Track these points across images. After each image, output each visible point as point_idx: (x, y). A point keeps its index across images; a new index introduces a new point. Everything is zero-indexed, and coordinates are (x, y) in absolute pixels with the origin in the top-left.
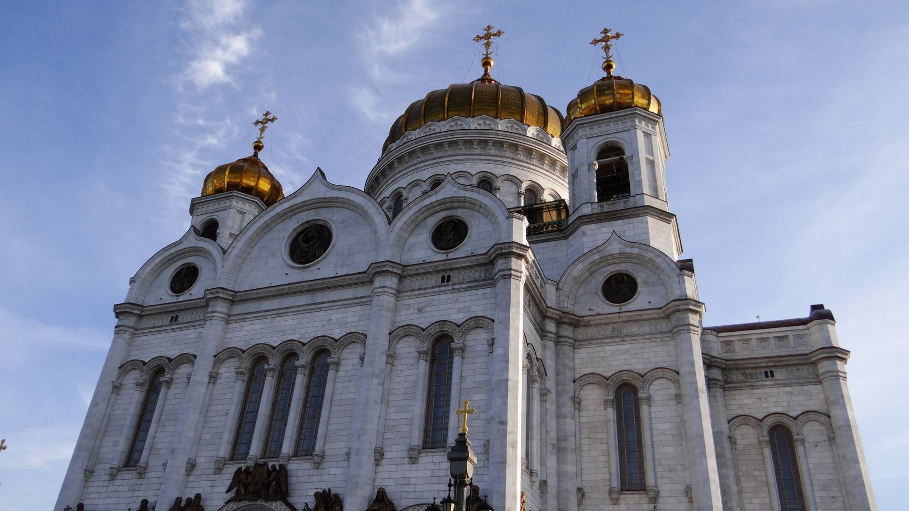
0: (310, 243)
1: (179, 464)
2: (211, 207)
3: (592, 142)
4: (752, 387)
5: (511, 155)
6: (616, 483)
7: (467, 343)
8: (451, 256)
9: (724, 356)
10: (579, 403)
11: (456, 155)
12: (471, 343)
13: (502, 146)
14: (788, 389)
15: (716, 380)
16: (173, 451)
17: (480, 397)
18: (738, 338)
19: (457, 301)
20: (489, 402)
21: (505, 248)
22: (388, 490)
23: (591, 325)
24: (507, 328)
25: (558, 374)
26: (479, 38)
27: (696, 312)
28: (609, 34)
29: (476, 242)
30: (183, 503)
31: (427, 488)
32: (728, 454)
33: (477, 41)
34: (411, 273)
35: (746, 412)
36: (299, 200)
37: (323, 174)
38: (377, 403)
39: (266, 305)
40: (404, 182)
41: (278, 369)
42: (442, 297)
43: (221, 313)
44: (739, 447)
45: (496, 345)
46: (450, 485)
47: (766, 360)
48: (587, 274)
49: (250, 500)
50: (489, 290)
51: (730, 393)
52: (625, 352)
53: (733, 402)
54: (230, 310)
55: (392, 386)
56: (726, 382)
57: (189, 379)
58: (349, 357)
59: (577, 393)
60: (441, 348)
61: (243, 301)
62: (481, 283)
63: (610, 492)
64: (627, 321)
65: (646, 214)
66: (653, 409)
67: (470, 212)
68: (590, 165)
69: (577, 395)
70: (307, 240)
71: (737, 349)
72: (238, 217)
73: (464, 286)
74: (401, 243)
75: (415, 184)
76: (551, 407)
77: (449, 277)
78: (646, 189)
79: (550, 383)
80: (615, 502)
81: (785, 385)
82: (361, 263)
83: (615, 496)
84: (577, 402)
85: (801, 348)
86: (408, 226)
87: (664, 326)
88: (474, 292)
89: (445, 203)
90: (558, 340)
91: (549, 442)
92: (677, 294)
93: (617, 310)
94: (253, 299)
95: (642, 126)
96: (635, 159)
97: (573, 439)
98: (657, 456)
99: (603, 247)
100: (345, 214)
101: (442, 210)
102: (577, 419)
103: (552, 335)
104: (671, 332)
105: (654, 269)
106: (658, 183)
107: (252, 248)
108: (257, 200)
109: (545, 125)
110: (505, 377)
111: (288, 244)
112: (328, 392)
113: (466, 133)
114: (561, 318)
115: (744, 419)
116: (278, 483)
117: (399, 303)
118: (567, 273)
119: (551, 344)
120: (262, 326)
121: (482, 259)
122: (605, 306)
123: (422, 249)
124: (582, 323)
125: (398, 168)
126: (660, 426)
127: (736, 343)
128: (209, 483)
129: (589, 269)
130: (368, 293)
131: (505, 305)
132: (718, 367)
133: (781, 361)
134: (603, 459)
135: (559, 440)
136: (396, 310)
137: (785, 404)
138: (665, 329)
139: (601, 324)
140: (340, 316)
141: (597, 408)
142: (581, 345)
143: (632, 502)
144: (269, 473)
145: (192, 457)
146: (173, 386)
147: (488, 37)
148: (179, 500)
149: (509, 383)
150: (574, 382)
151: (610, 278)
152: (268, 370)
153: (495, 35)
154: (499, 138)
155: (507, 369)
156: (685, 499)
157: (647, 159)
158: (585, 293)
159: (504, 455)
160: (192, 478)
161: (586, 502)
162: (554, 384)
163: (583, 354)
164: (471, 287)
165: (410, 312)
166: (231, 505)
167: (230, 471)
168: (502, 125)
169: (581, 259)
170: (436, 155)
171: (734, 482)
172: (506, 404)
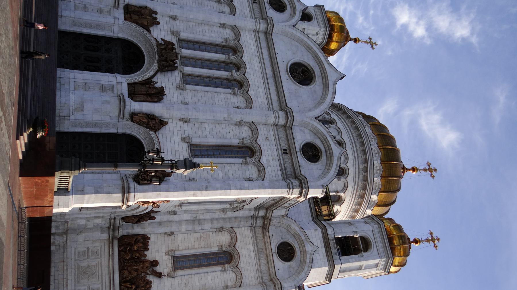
0: (302, 74)
1: (176, 12)
2: (319, 17)
5: (360, 186)
6: (177, 253)
7: (250, 166)
8: (299, 154)
10: (220, 231)
11: (357, 154)
12: (250, 168)
13: (364, 181)
16: (182, 7)
17: (220, 175)
19: (273, 159)
20: (217, 180)
21: (305, 185)
22: (166, 127)
23: (264, 236)
24: (259, 188)
25: (235, 218)
26: (429, 164)
28: (436, 242)
29: (307, 168)
30: (154, 16)
31: (169, 148)
33: (427, 164)
34: (288, 132)
36: (326, 65)
37: (342, 78)
38: (214, 117)
39: (265, 52)
40: (340, 125)
41: (230, 61)
42: (275, 150)
43: (259, 27)
45: (249, 182)
46: (171, 160)
48: (293, 233)
49: (158, 52)
50: (280, 176)
52: (250, 256)
54: (261, 32)
55: (224, 126)
57: (222, 12)
58: (238, 100)
59: (225, 229)
60: (246, 151)
61: (267, 39)
62: (284, 172)
63: (172, 251)
64: (267, 257)
65: (330, 266)
66: (219, 273)
67: (325, 164)
68: (356, 232)
69: (224, 229)
70: (303, 72)
72: (314, 32)
73: (282, 162)
74: (305, 125)
75: (339, 131)
76: (217, 215)
77: (287, 154)
78: (344, 266)
79: (230, 214)
80: (167, 254)
82: (291, 103)
83: (170, 253)
84: (220, 230)
86: (314, 129)
87: (266, 278)
88: (279, 168)
89: (329, 149)
90: (254, 218)
91: (198, 215)
93: (274, 250)
94: (268, 44)
95: (382, 262)
96: (362, 258)
97: (200, 228)
98: (193, 276)
99: (309, 241)
100: (320, 92)
101: (325, 148)
102: (211, 230)
103: (257, 214)
104: (263, 282)
105: (298, 271)
106: (348, 273)
107: (297, 41)
108: (325, 42)
109: (378, 205)
110: (232, 188)
111: (300, 61)
112: (219, 90)
113: (371, 159)
114: (267, 219)
116: (168, 66)
117: (270, 127)
118: (293, 221)
119: (252, 213)
120: (253, 50)
121: (298, 172)
122: (275, 243)
123: (301, 137)
125: (348, 121)
126: (210, 277)
128: (166, 28)
129: (296, 234)
130: (275, 108)
131: (272, 187)
134: (190, 245)
135: (199, 220)
136: (266, 124)
138: (264, 278)
139: (265, 242)
140: (261, 94)
141: (217, 242)
142: (252, 231)
143: (167, 263)
144: (173, 61)
145: (179, 18)
146: (217, 4)
147: (430, 170)
148: (156, 13)
149: (229, 191)
150: (232, 228)
152: (229, 56)
153: (432, 174)
154: (369, 179)
155: (237, 189)
157: (362, 266)
158: (281, 232)
159: (189, 190)
160: (168, 19)
161: (166, 237)
165: (266, 133)
166: (155, 41)
167: (172, 39)
168: (377, 180)
169: (301, 229)
170: (357, 143)
172: (217, 189)
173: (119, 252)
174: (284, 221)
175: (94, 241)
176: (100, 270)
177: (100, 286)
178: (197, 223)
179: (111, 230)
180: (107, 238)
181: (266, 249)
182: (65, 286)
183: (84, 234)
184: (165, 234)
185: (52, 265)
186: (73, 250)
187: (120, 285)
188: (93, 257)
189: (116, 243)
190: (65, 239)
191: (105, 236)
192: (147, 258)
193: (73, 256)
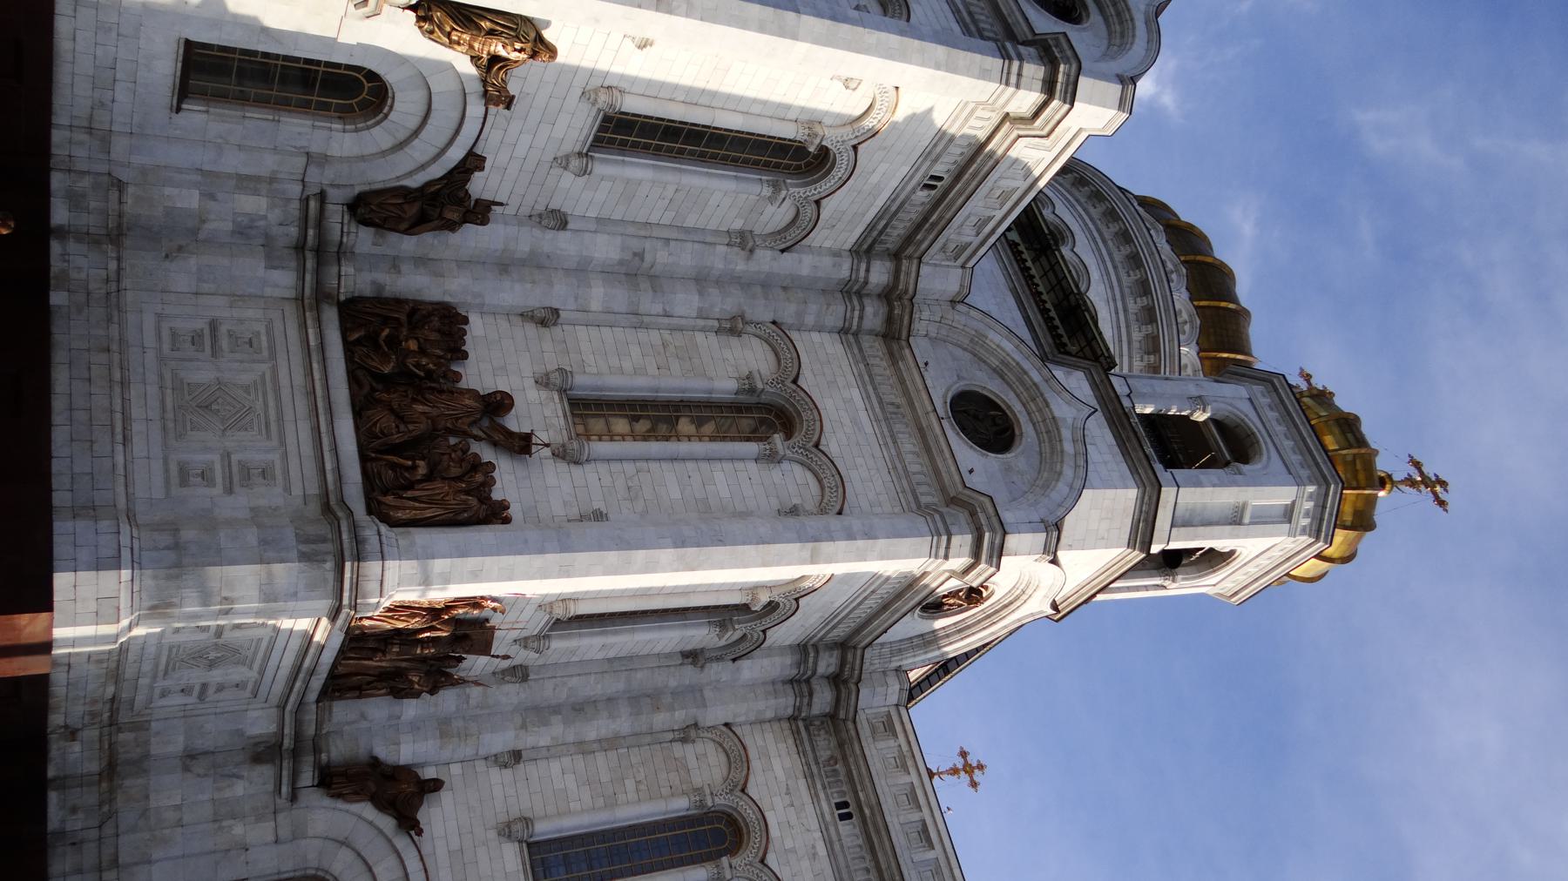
3: (1246, 407)
4: (809, 776)
9: (861, 717)
10: (734, 332)
11: (1115, 267)
14: (822, 850)
15: (811, 695)
18: (905, 748)
21: (1062, 51)
27: (976, 554)
28: (1438, 489)
32: (661, 720)
35: (756, 764)
44: (678, 749)
47: (874, 801)
48: (995, 362)
51: (787, 732)
52: (855, 422)
53: (769, 736)
56: (809, 723)
59: (750, 329)
64: (921, 430)
65: (1141, 484)
66: (752, 466)
68: (1200, 401)
71: (881, 745)
76: (722, 259)
79: (766, 261)
80: (543, 382)
81: (829, 844)
84: (733, 327)
85: (913, 873)
90: (852, 291)
91: (648, 245)
92: (1007, 517)
93: (941, 413)
97: (657, 308)
98: (654, 466)
99: (1059, 388)
102: (701, 323)
103: (862, 274)
113: (1160, 281)
114: (900, 298)
115: (738, 760)
118: (988, 320)
119: (845, 272)
124: (895, 347)
126: (719, 476)
127: (892, 743)
129: (1007, 365)
132: (838, 700)
133: (878, 832)
134: (627, 365)
137: (789, 844)
139: (902, 382)
142: (850, 346)
149: (791, 15)
151: (996, 407)
154: (1165, 346)
156: (574, 512)
157: (1244, 506)
158: (955, 359)
161: (531, 329)
162: (766, 268)
163: (832, 347)
164: (959, 11)
171: (604, 733)
173: (349, 348)
174: (958, 317)
175: (237, 299)
176: (271, 403)
177: (275, 457)
178: (645, 285)
179: (309, 255)
180: (291, 294)
181: (911, 404)
182: (119, 438)
183: (193, 261)
184: (528, 316)
185: (59, 357)
186: (149, 323)
187: (364, 459)
188: (238, 356)
189: (331, 316)
190: (113, 265)
191: (283, 280)
192: (463, 384)
193: (150, 340)
